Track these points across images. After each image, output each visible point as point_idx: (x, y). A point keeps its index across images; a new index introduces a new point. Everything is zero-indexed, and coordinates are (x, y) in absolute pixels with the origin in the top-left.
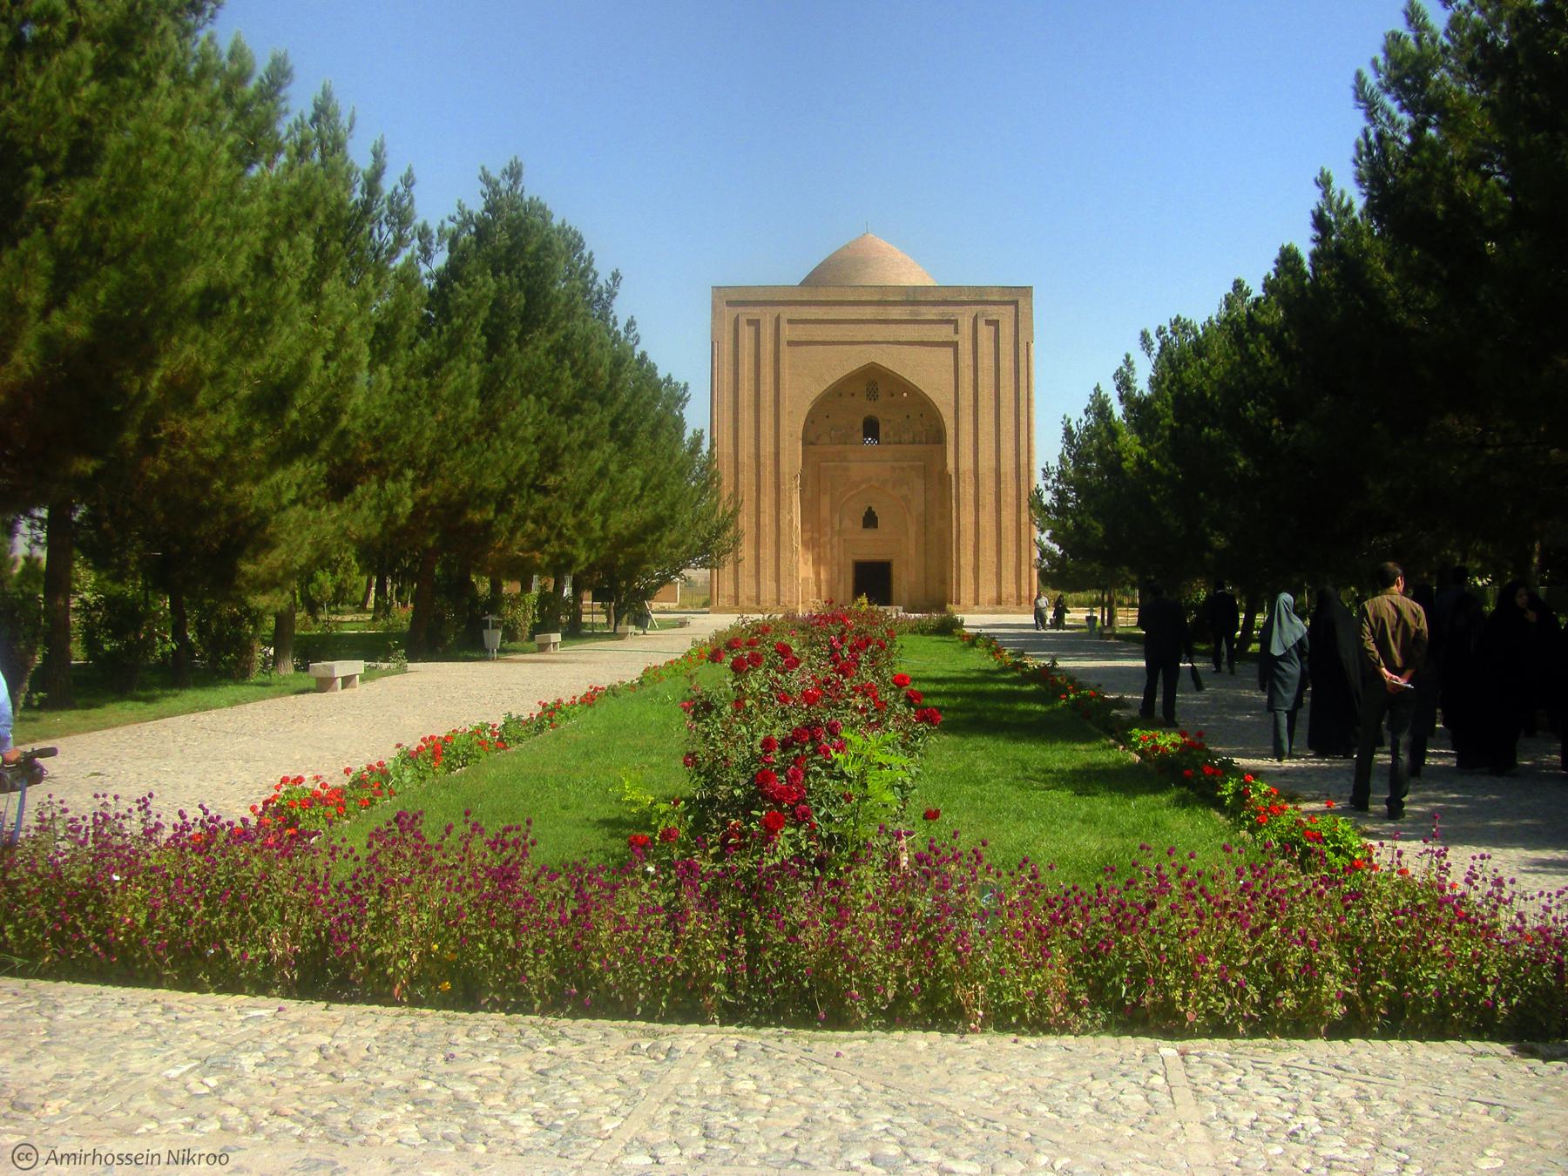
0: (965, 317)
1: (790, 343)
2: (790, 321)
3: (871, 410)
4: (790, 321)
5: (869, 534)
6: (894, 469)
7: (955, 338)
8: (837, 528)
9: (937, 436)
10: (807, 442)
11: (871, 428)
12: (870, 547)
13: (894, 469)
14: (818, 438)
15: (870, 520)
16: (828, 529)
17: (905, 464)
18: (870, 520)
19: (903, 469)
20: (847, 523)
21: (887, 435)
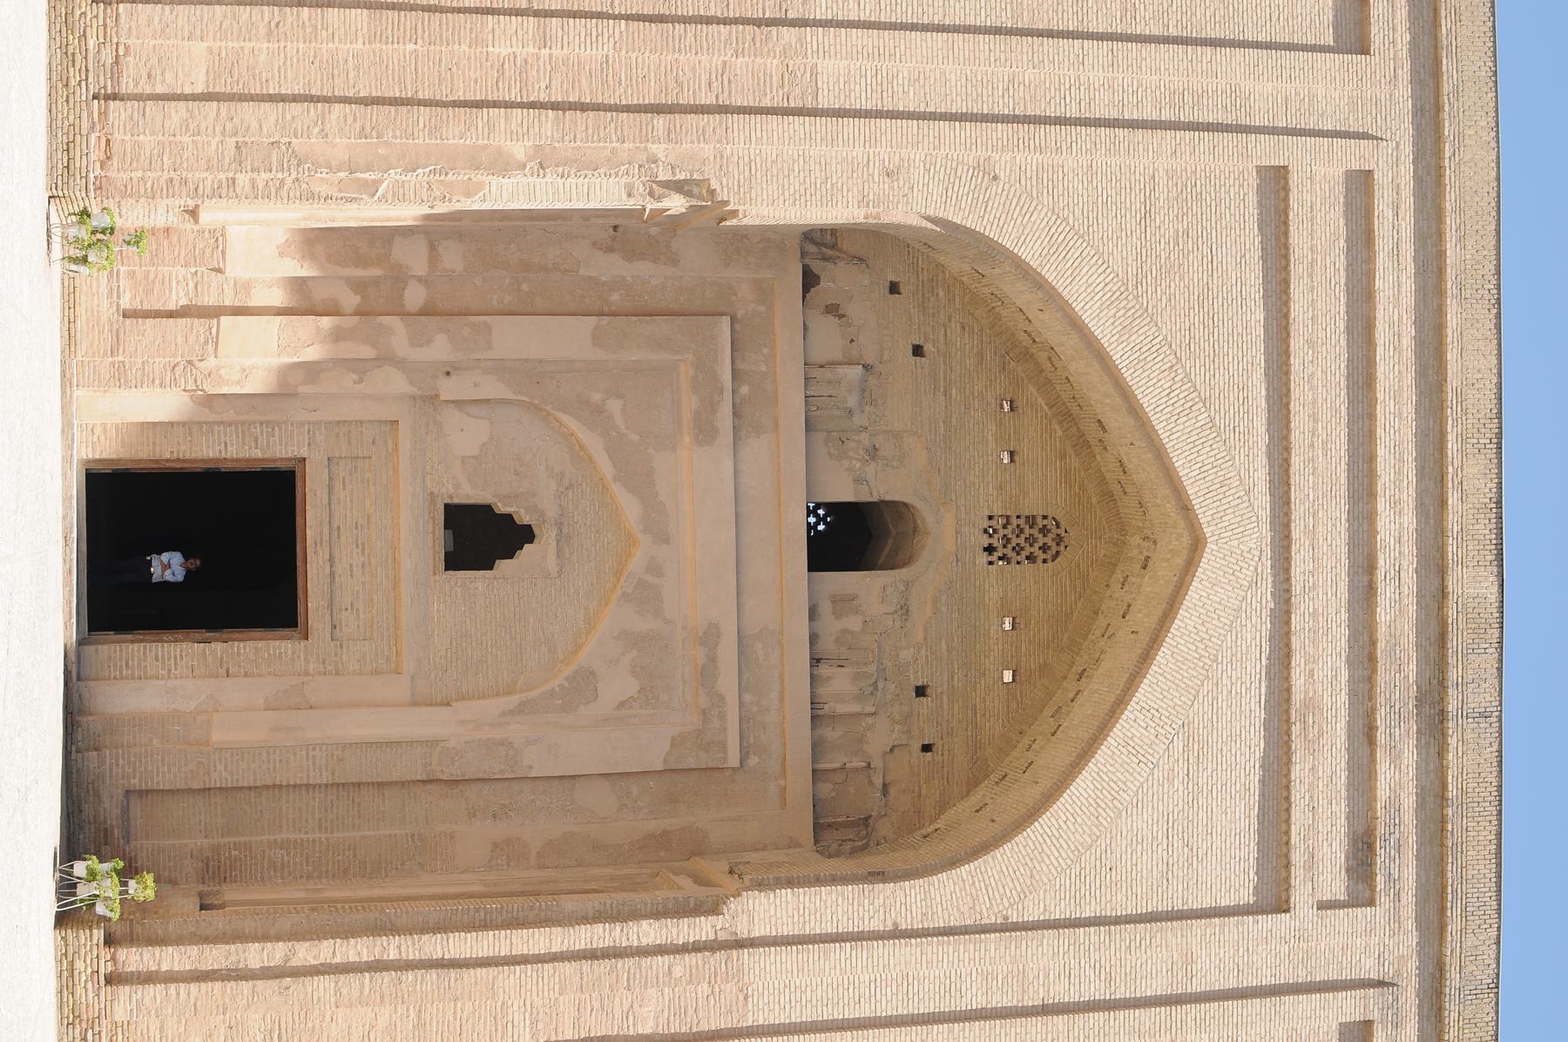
0: (1381, 939)
1: (1275, 183)
2: (1360, 185)
3: (948, 535)
4: (1360, 185)
5: (423, 539)
6: (709, 638)
7: (1301, 896)
8: (449, 389)
9: (856, 826)
10: (818, 251)
11: (849, 537)
12: (362, 545)
13: (709, 638)
14: (832, 309)
15: (480, 538)
16: (440, 349)
17: (727, 682)
18: (480, 538)
19: (707, 673)
20: (467, 435)
21: (844, 604)
